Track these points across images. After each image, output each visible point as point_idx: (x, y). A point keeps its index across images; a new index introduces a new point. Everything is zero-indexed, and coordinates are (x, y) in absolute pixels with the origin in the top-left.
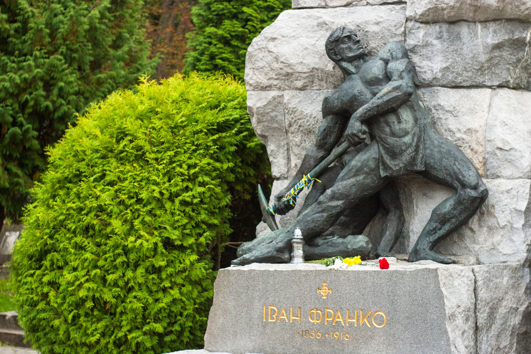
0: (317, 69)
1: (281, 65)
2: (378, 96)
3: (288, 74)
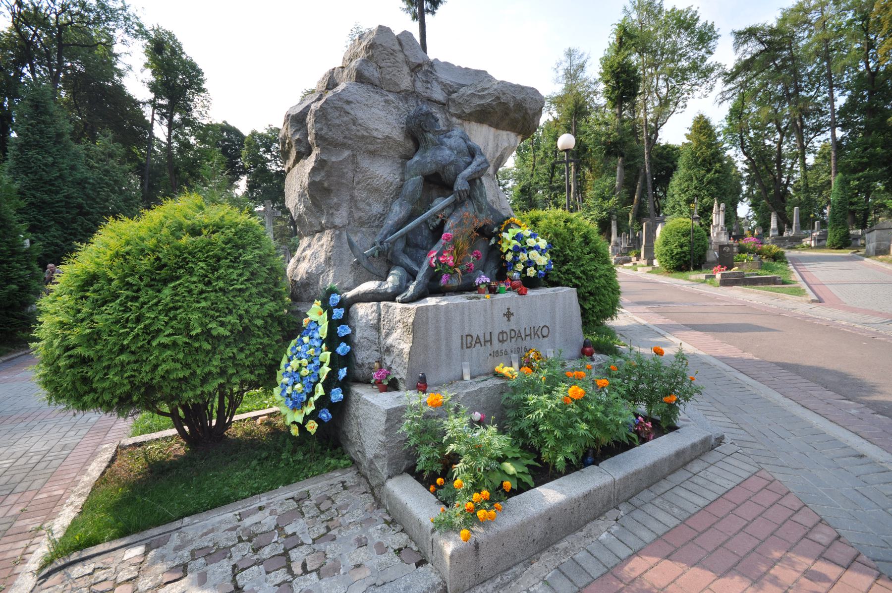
0: (390, 138)
2: (474, 164)
3: (363, 137)
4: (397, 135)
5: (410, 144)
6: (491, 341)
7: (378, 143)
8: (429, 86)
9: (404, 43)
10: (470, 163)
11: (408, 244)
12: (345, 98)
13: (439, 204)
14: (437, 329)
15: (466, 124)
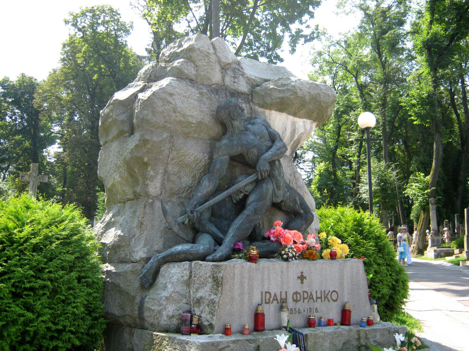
3: (180, 122)
4: (208, 120)
8: (236, 80)
9: (217, 47)
10: (271, 147)
11: (213, 215)
14: (242, 284)
15: (267, 112)
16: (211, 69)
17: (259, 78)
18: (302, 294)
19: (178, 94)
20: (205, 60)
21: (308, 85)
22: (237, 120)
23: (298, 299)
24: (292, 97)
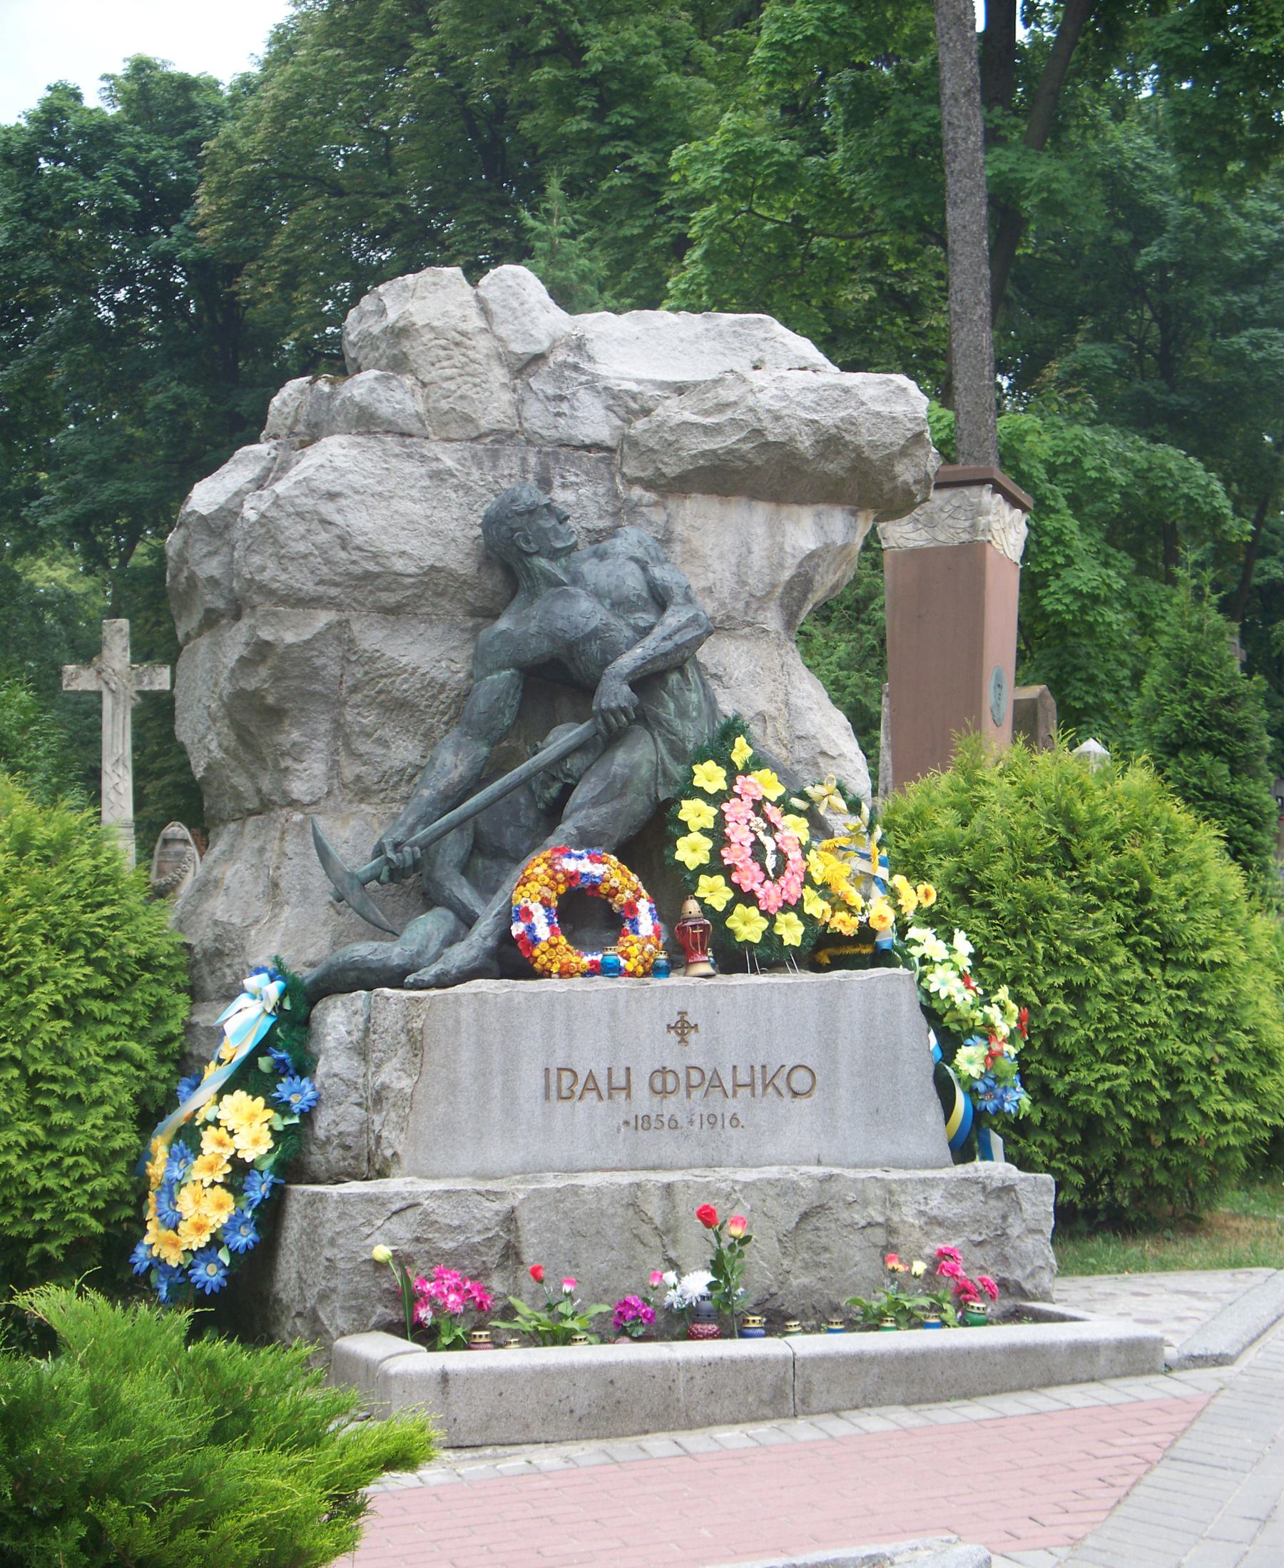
1: (356, 555)
2: (658, 632)
3: (368, 576)
5: (493, 581)
6: (628, 1088)
7: (407, 587)
8: (565, 407)
9: (493, 307)
10: (645, 632)
12: (324, 487)
13: (563, 737)
15: (672, 504)
16: (475, 385)
17: (653, 382)
18: (682, 1076)
19: (357, 492)
20: (449, 358)
21: (812, 396)
22: (537, 553)
23: (670, 1087)
24: (746, 447)
